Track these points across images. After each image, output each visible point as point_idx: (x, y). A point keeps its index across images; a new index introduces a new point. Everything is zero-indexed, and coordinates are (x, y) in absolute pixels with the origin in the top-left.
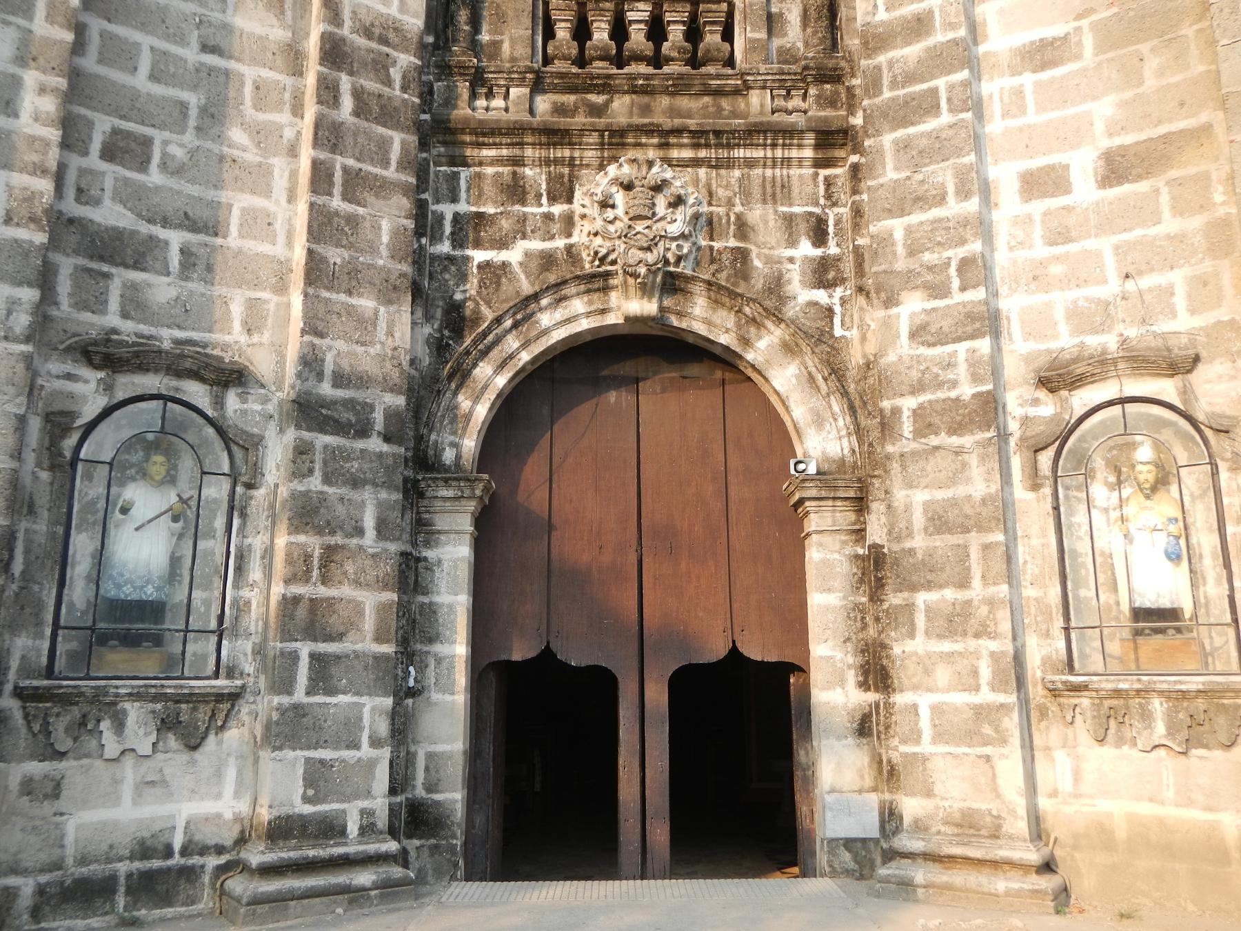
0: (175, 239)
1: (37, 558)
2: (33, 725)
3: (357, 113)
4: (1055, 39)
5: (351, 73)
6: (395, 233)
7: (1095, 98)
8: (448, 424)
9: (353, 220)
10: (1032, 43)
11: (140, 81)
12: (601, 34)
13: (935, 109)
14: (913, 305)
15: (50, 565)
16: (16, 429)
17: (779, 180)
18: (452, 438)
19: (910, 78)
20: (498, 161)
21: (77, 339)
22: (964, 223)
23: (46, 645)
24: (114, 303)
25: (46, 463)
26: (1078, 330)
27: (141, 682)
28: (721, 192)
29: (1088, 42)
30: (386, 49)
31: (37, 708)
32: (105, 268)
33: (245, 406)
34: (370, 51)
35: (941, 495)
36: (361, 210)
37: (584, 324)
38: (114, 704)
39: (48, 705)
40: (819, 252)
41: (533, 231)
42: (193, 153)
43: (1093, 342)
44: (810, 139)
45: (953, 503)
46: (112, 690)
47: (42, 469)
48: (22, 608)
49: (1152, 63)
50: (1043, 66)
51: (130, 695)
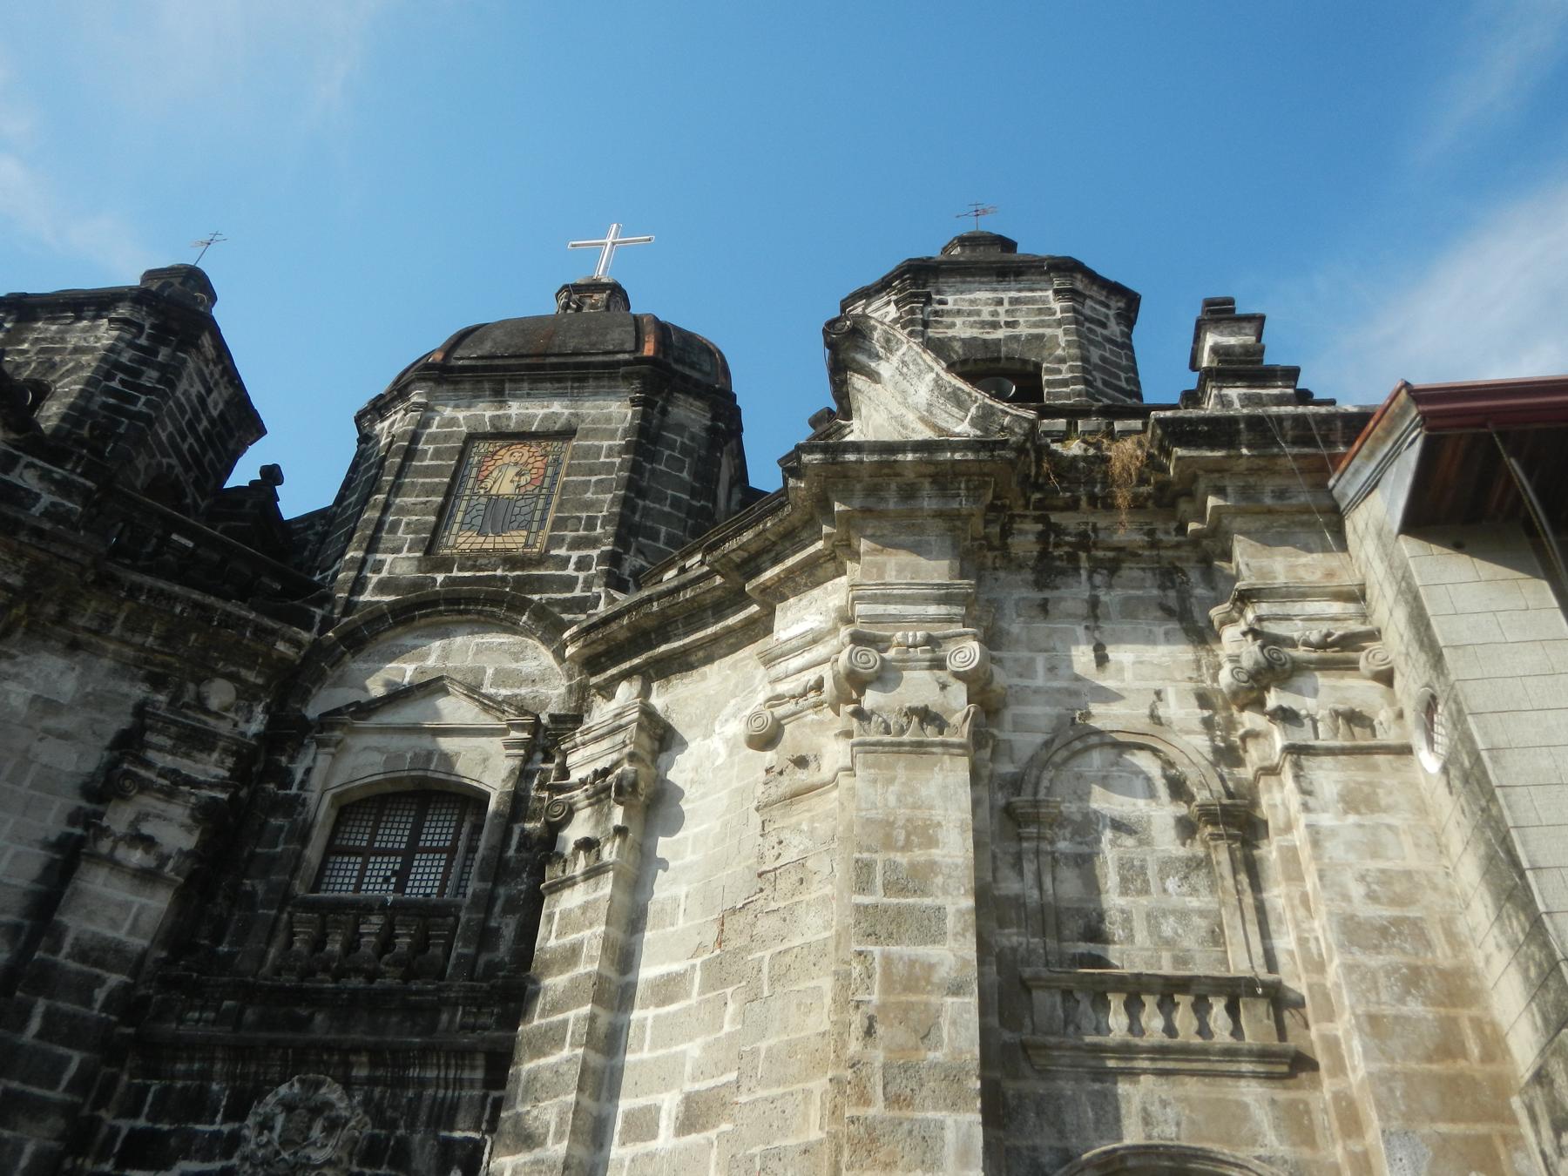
4: (678, 974)
5: (50, 996)
6: (37, 1156)
10: (662, 976)
12: (335, 946)
13: (558, 1043)
17: (448, 1101)
20: (188, 1075)
28: (389, 1113)
30: (98, 971)
34: (79, 973)
41: (197, 1151)
44: (480, 1060)
50: (663, 1002)
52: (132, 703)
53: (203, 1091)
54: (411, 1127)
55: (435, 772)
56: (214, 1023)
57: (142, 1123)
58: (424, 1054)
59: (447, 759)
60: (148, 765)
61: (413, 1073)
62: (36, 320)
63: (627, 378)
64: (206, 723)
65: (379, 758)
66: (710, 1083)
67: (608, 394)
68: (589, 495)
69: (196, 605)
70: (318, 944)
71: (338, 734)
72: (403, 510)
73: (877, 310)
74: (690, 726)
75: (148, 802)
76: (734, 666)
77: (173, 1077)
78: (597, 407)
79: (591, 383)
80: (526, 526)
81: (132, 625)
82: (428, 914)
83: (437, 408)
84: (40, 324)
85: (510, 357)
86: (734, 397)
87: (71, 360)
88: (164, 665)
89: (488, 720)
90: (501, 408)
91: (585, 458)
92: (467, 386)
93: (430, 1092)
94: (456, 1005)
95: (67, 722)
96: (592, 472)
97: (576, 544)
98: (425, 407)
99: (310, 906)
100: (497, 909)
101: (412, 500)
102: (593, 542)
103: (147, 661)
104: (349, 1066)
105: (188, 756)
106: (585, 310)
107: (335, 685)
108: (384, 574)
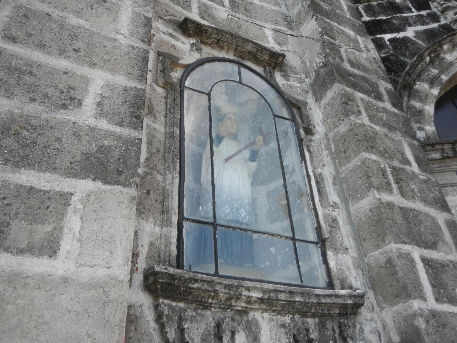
1: (158, 151)
2: (167, 329)
8: (411, 117)
15: (171, 158)
16: (145, 26)
18: (418, 125)
21: (175, 18)
23: (175, 233)
25: (161, 81)
27: (271, 286)
31: (171, 307)
33: (289, 83)
38: (244, 312)
39: (182, 305)
46: (245, 293)
47: (158, 85)
48: (148, 193)
51: (261, 300)
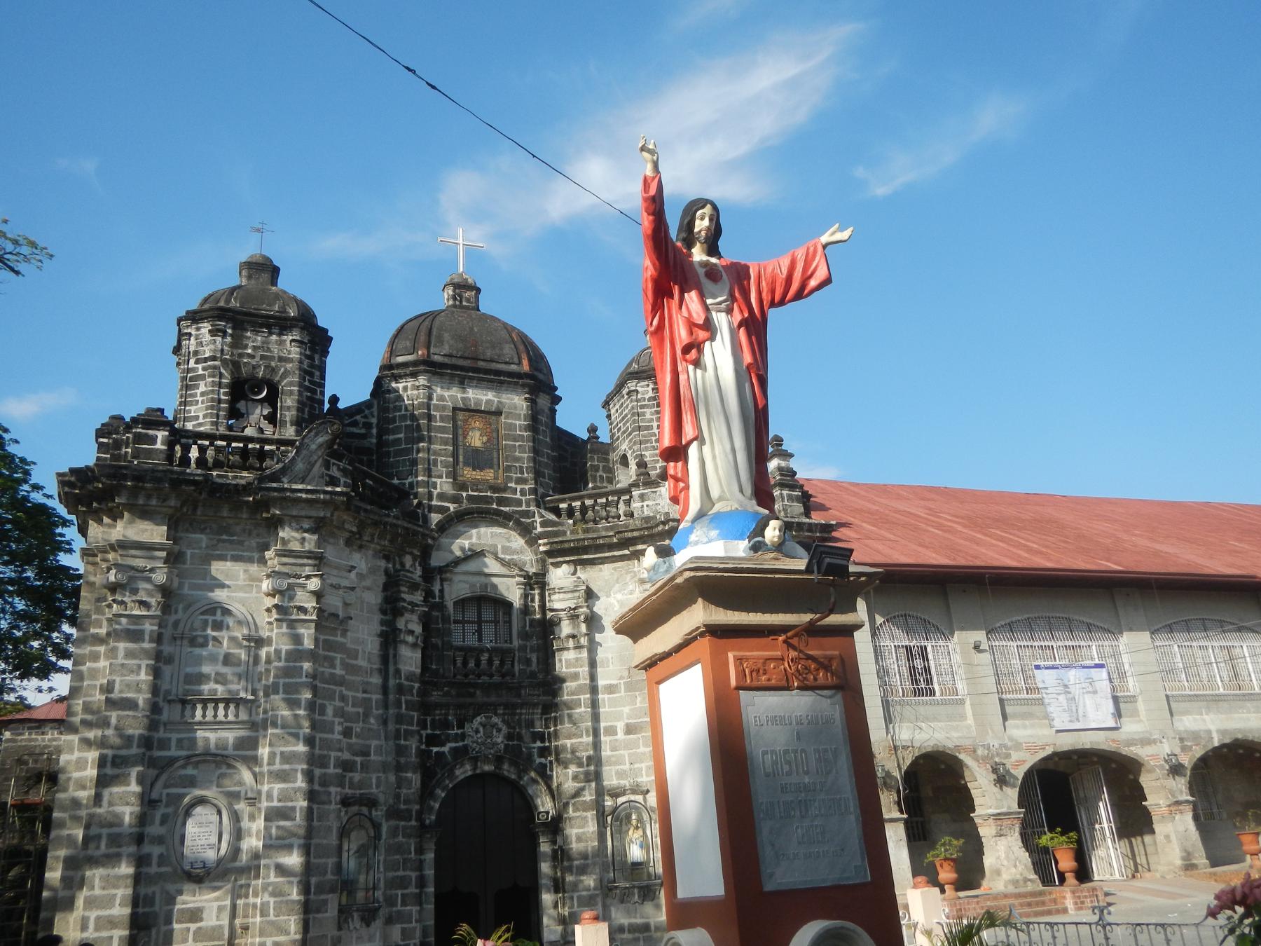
0: (358, 759)
3: (406, 709)
7: (624, 706)
9: (406, 747)
11: (350, 709)
12: (472, 664)
14: (573, 769)
19: (573, 694)
20: (441, 714)
22: (588, 744)
24: (347, 786)
26: (618, 779)
28: (512, 724)
29: (623, 687)
32: (344, 774)
34: (409, 685)
35: (581, 830)
36: (408, 743)
37: (470, 773)
40: (542, 745)
42: (362, 728)
43: (623, 782)
44: (540, 707)
45: (583, 833)
49: (639, 699)
52: (382, 570)
53: (446, 720)
54: (520, 728)
55: (490, 593)
56: (443, 696)
57: (429, 731)
58: (522, 706)
59: (495, 587)
60: (404, 600)
61: (518, 711)
62: (246, 330)
63: (523, 386)
64: (412, 579)
65: (468, 586)
66: (635, 721)
67: (512, 391)
68: (517, 453)
69: (407, 529)
70: (465, 663)
71: (448, 575)
72: (436, 453)
73: (642, 387)
74: (600, 591)
75: (407, 616)
76: (615, 569)
77: (434, 715)
78: (508, 399)
79: (506, 385)
80: (491, 467)
81: (380, 537)
82: (504, 654)
83: (434, 387)
84: (249, 334)
85: (461, 357)
86: (556, 389)
87: (281, 366)
88: (389, 551)
89: (504, 571)
90: (464, 393)
91: (511, 430)
92: (447, 378)
93: (523, 717)
94: (525, 687)
95: (368, 583)
96: (515, 440)
97: (519, 481)
98: (429, 387)
99: (460, 649)
100: (528, 651)
101: (439, 447)
102: (524, 481)
103: (383, 550)
104: (496, 710)
105: (412, 594)
106: (464, 303)
107: (438, 550)
108: (439, 490)
